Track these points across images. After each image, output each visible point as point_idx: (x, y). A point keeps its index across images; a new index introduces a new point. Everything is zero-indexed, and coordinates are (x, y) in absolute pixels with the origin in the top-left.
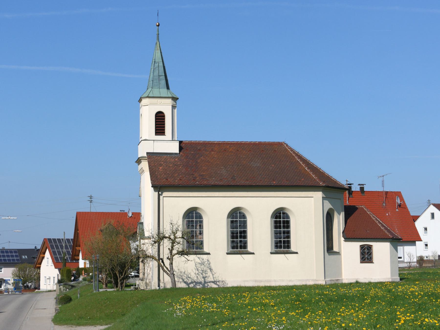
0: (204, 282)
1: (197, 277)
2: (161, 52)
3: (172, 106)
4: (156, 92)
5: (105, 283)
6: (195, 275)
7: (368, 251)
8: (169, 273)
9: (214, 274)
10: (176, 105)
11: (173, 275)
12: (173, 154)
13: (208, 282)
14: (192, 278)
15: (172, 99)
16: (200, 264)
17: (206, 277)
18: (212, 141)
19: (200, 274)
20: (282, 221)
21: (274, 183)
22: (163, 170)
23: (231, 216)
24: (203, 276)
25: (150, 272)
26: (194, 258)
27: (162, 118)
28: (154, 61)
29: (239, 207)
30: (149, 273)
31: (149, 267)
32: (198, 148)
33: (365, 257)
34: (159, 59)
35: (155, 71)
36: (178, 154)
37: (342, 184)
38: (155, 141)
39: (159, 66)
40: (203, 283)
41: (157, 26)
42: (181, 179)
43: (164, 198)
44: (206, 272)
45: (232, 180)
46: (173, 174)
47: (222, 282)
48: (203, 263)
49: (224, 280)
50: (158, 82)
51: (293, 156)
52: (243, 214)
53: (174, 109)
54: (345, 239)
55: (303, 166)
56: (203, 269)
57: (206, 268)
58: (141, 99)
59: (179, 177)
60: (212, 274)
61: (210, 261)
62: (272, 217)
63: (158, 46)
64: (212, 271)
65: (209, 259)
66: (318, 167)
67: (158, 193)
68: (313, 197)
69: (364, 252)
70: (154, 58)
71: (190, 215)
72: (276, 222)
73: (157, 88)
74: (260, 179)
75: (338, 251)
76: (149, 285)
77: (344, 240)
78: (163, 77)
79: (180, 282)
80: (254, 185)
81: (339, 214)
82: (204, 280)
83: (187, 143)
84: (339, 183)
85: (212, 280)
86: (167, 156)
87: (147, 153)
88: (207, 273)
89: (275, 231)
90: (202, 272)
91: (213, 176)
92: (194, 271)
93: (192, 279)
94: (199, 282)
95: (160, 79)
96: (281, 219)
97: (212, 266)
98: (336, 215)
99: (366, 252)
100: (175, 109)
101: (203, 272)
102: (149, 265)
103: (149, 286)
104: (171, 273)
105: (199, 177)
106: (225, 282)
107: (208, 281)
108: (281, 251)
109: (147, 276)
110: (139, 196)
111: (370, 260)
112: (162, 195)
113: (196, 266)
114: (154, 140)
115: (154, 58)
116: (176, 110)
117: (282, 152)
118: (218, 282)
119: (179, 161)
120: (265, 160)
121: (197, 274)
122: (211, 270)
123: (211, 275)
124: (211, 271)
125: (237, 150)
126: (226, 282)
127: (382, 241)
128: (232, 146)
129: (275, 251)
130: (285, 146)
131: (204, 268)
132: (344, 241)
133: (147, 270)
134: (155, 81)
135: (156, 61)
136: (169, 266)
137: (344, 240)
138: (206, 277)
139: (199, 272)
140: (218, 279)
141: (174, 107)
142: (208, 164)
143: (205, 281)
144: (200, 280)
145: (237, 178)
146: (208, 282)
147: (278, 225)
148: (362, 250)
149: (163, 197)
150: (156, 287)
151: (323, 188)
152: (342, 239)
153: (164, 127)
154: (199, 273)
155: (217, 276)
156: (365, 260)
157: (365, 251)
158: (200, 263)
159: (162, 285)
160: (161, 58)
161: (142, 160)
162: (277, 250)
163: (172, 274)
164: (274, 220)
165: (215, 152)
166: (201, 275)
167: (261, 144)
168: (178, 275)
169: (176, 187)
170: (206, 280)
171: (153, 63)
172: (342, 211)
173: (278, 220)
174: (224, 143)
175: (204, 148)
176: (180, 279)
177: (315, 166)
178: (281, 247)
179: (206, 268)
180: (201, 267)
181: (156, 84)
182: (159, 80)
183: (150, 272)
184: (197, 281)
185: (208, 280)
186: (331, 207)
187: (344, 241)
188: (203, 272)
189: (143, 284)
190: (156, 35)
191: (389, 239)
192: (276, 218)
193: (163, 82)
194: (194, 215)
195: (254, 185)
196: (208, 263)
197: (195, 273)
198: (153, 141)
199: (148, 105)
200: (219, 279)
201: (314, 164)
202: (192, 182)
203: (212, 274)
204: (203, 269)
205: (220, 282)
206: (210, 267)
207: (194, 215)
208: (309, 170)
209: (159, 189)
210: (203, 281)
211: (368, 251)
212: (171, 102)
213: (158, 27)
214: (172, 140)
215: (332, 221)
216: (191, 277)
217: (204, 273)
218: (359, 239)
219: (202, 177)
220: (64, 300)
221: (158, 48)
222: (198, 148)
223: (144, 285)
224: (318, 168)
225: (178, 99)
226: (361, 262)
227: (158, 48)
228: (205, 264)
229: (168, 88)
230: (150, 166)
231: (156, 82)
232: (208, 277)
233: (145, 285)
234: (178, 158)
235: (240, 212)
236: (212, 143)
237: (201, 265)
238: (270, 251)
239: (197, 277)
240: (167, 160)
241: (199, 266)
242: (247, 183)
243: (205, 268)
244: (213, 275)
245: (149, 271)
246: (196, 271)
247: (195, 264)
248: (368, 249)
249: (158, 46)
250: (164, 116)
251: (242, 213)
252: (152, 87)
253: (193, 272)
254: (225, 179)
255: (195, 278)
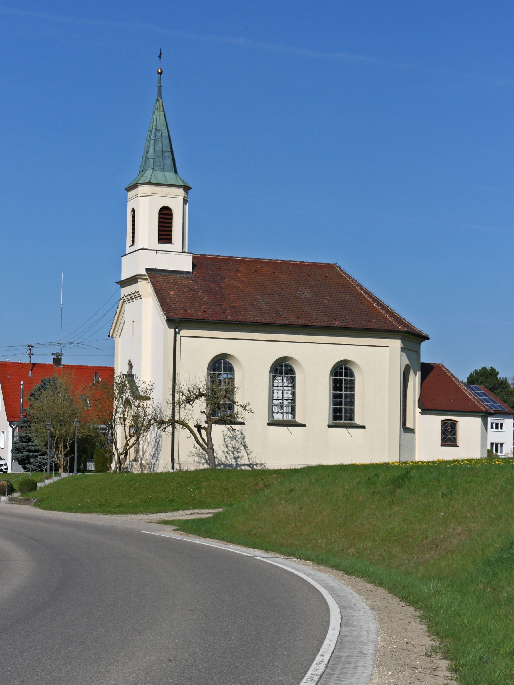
0: (236, 465)
1: (226, 457)
2: (165, 115)
3: (183, 199)
4: (159, 176)
5: (63, 466)
6: (223, 454)
7: (451, 429)
8: (206, 447)
9: (250, 453)
10: (187, 198)
11: (212, 450)
12: (185, 274)
13: (241, 465)
14: (219, 458)
15: (183, 189)
16: (230, 438)
17: (239, 457)
18: (234, 256)
19: (230, 452)
20: (343, 380)
21: (337, 323)
22: (176, 296)
23: (273, 369)
24: (235, 455)
25: (147, 449)
26: (222, 429)
27: (168, 217)
28: (154, 127)
29: (290, 357)
30: (146, 450)
31: (147, 441)
32: (217, 266)
33: (447, 437)
34: (161, 126)
35: (157, 145)
36: (191, 274)
37: (420, 331)
38: (158, 252)
39: (162, 136)
40: (235, 466)
41: (159, 73)
42: (205, 310)
43: (182, 337)
44: (239, 450)
45: (277, 316)
46: (193, 303)
47: (261, 465)
48: (235, 437)
49: (263, 462)
50: (162, 160)
51: (353, 286)
52: (290, 367)
53: (185, 205)
54: (422, 410)
55: (370, 300)
56: (235, 445)
57: (238, 444)
58: (136, 185)
59: (201, 308)
60: (247, 453)
61: (245, 434)
62: (331, 374)
63: (160, 105)
64: (247, 449)
65: (243, 432)
66: (385, 304)
67: (175, 330)
68: (388, 347)
69: (447, 430)
70: (155, 122)
71: (217, 365)
72: (335, 381)
73: (161, 171)
74: (316, 317)
75: (412, 428)
76: (146, 467)
77: (421, 411)
78: (169, 154)
79: (203, 463)
80: (310, 325)
81: (416, 375)
82: (236, 461)
83: (198, 257)
84: (415, 329)
85: (247, 462)
86: (177, 276)
87: (147, 270)
88: (240, 452)
89: (333, 394)
90: (233, 450)
91: (249, 309)
92: (222, 447)
93: (219, 460)
94: (229, 464)
95: (164, 156)
96: (342, 376)
97: (247, 442)
98: (412, 374)
99: (449, 431)
100: (186, 205)
101: (235, 450)
102: (147, 438)
103: (146, 470)
104: (209, 447)
105: (230, 310)
106: (264, 465)
107: (242, 464)
108: (341, 423)
109: (143, 455)
110: (109, 336)
111: (453, 442)
112: (179, 334)
113: (225, 441)
114: (157, 250)
115: (155, 122)
116: (187, 206)
117: (336, 279)
118: (255, 465)
119: (195, 283)
120: (315, 289)
121: (225, 452)
122: (245, 447)
123: (245, 454)
124: (246, 449)
125: (272, 273)
126: (266, 465)
127: (470, 415)
128: (264, 265)
129: (334, 423)
130: (338, 270)
131: (236, 445)
132: (420, 413)
133: (143, 446)
134: (157, 160)
135: (158, 128)
136: (206, 437)
137: (421, 411)
138: (239, 457)
139: (229, 450)
140: (255, 461)
141: (185, 201)
142: (237, 290)
143: (236, 463)
144: (231, 462)
145: (282, 313)
146: (241, 465)
147: (338, 385)
148: (444, 428)
149: (181, 336)
150: (168, 470)
151: (403, 334)
152: (418, 410)
153: (171, 231)
154: (228, 451)
155: (254, 457)
156: (447, 441)
157: (448, 429)
158: (231, 437)
159: (177, 466)
160: (165, 124)
161: (139, 280)
162: (335, 421)
163: (211, 449)
164: (332, 378)
165: (242, 273)
166: (232, 454)
167: (305, 265)
168: (200, 453)
169: (220, 323)
170: (238, 461)
171: (154, 131)
172: (419, 371)
173: (338, 378)
174: (252, 261)
175: (225, 266)
176: (203, 459)
177: (381, 302)
178: (340, 418)
179: (238, 444)
180: (232, 442)
181: (158, 164)
182: (164, 158)
183: (147, 448)
184: (226, 463)
185: (241, 461)
186: (409, 363)
187: (420, 413)
188: (234, 451)
189: (137, 465)
190: (157, 88)
191: (482, 412)
192: (335, 376)
193: (169, 162)
194: (222, 365)
195: (310, 325)
196: (241, 437)
197: (223, 452)
198: (156, 251)
199: (148, 196)
200: (256, 461)
201: (378, 299)
202: (222, 316)
203: (247, 453)
204: (234, 446)
205: (258, 465)
206: (244, 442)
207: (222, 365)
208: (380, 307)
209: (177, 324)
210: (235, 464)
211: (451, 429)
212: (182, 193)
213: (160, 75)
214: (183, 252)
215: (406, 384)
216: (218, 456)
217: (236, 451)
218: (441, 411)
219: (234, 310)
220: (27, 486)
221: (160, 109)
222: (217, 266)
223: (138, 467)
224: (385, 305)
225: (191, 188)
226: (442, 445)
227: (160, 109)
228: (237, 439)
229: (176, 172)
230: (157, 290)
231: (159, 161)
232: (241, 457)
233: (140, 467)
234: (192, 279)
235: (287, 364)
236: (234, 260)
237: (232, 440)
238: (327, 423)
239: (226, 457)
240: (177, 282)
241: (229, 442)
242: (299, 321)
243: (238, 445)
244: (248, 455)
245: (145, 447)
246: (224, 447)
247: (224, 437)
248: (452, 427)
249: (160, 105)
250: (171, 214)
251: (289, 365)
252: (153, 169)
253: (221, 449)
254: (267, 314)
255: (224, 459)
